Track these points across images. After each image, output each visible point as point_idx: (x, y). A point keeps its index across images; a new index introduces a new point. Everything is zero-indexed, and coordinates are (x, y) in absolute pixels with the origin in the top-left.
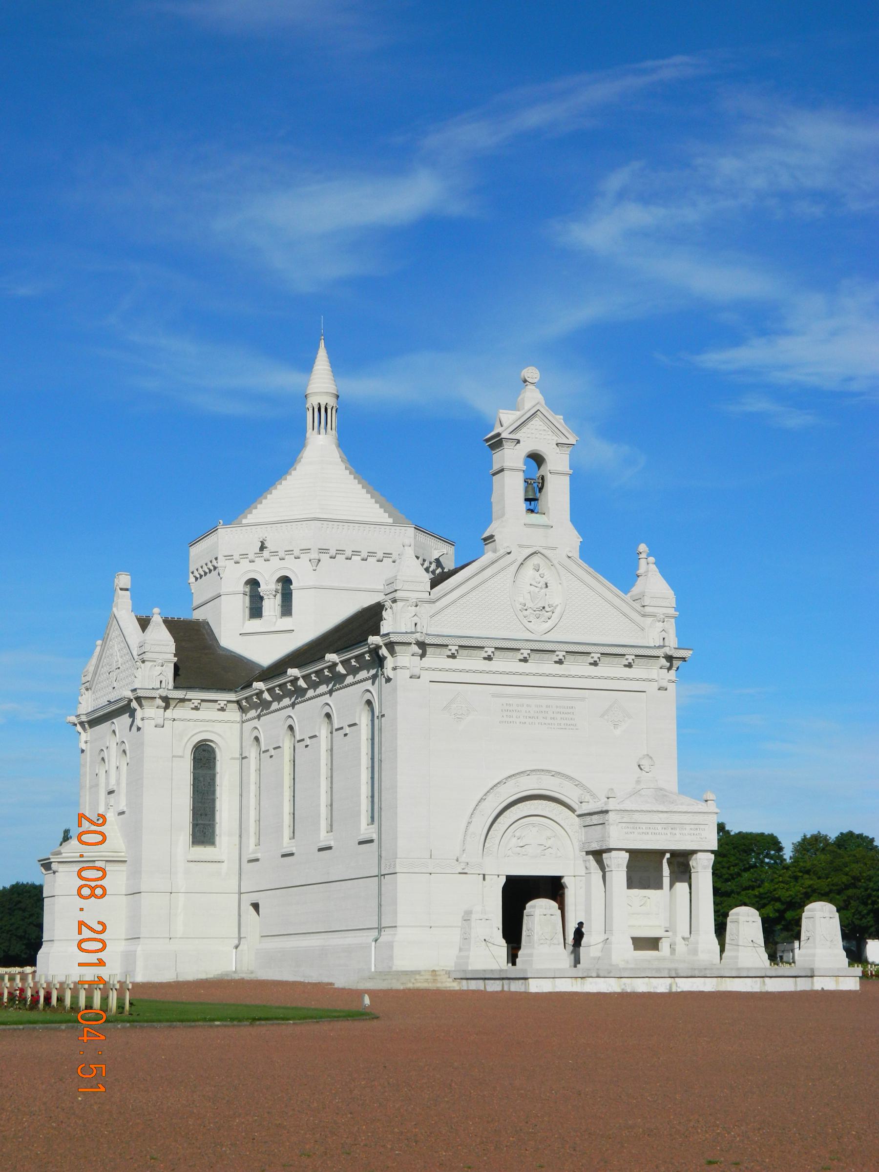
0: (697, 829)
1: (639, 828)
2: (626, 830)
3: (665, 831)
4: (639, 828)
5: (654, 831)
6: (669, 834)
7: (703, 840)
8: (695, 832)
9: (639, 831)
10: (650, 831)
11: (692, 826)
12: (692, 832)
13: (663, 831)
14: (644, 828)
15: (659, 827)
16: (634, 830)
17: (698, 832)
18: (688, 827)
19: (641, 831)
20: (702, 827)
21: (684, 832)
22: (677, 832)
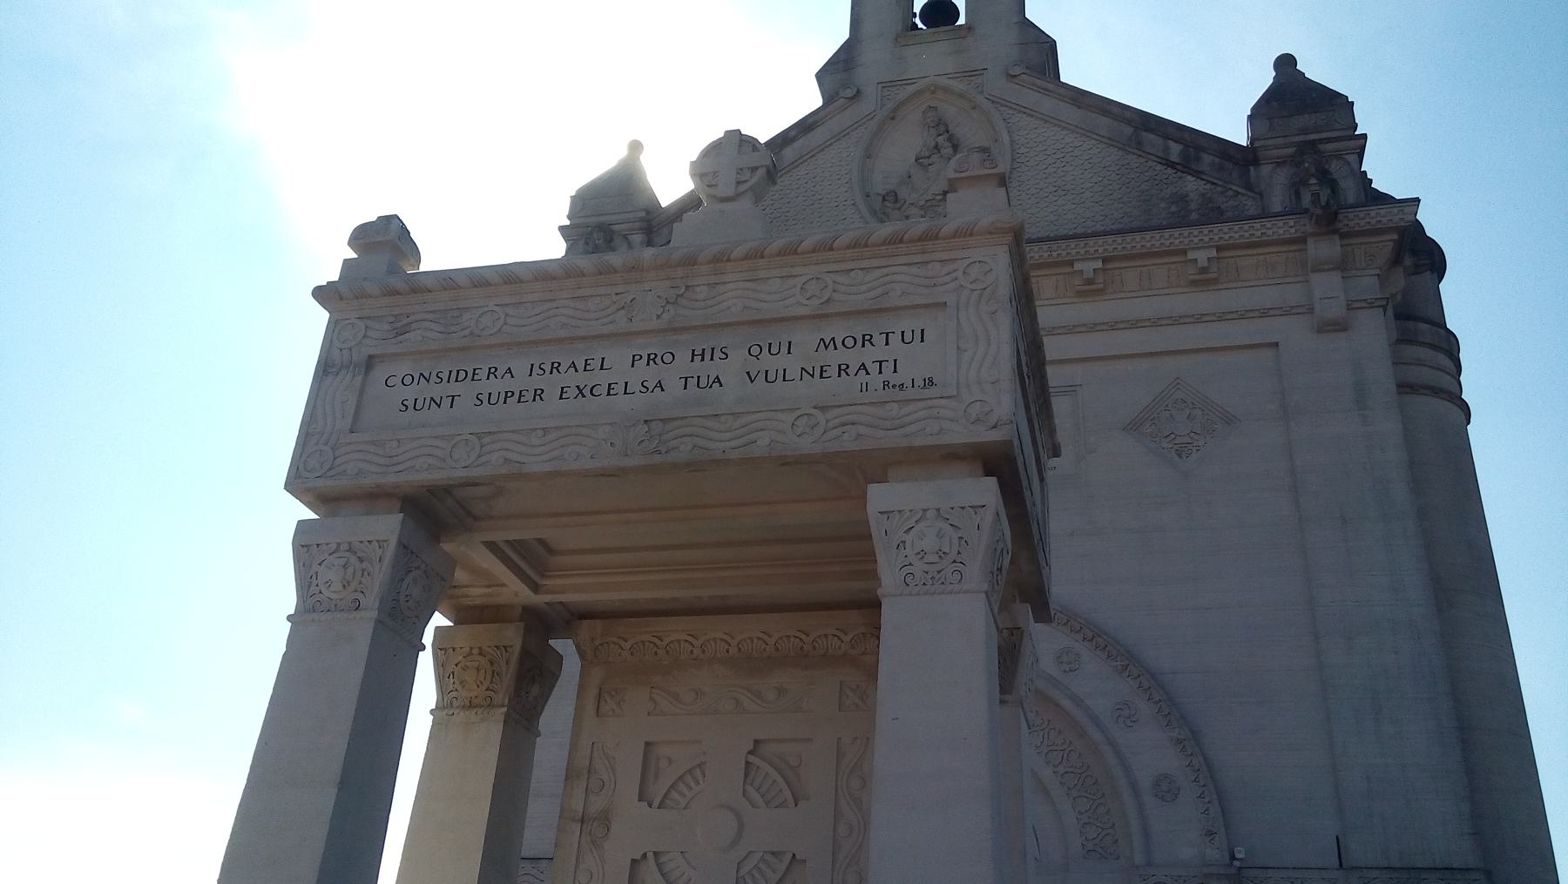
0: (867, 339)
1: (492, 372)
2: (410, 393)
3: (650, 374)
4: (492, 372)
5: (571, 379)
6: (674, 385)
7: (910, 393)
8: (853, 358)
9: (497, 386)
10: (551, 384)
11: (838, 331)
12: (835, 357)
13: (644, 372)
14: (520, 366)
15: (618, 357)
16: (455, 388)
17: (869, 355)
18: (806, 339)
19: (497, 386)
20: (907, 324)
21: (769, 362)
22: (731, 369)
